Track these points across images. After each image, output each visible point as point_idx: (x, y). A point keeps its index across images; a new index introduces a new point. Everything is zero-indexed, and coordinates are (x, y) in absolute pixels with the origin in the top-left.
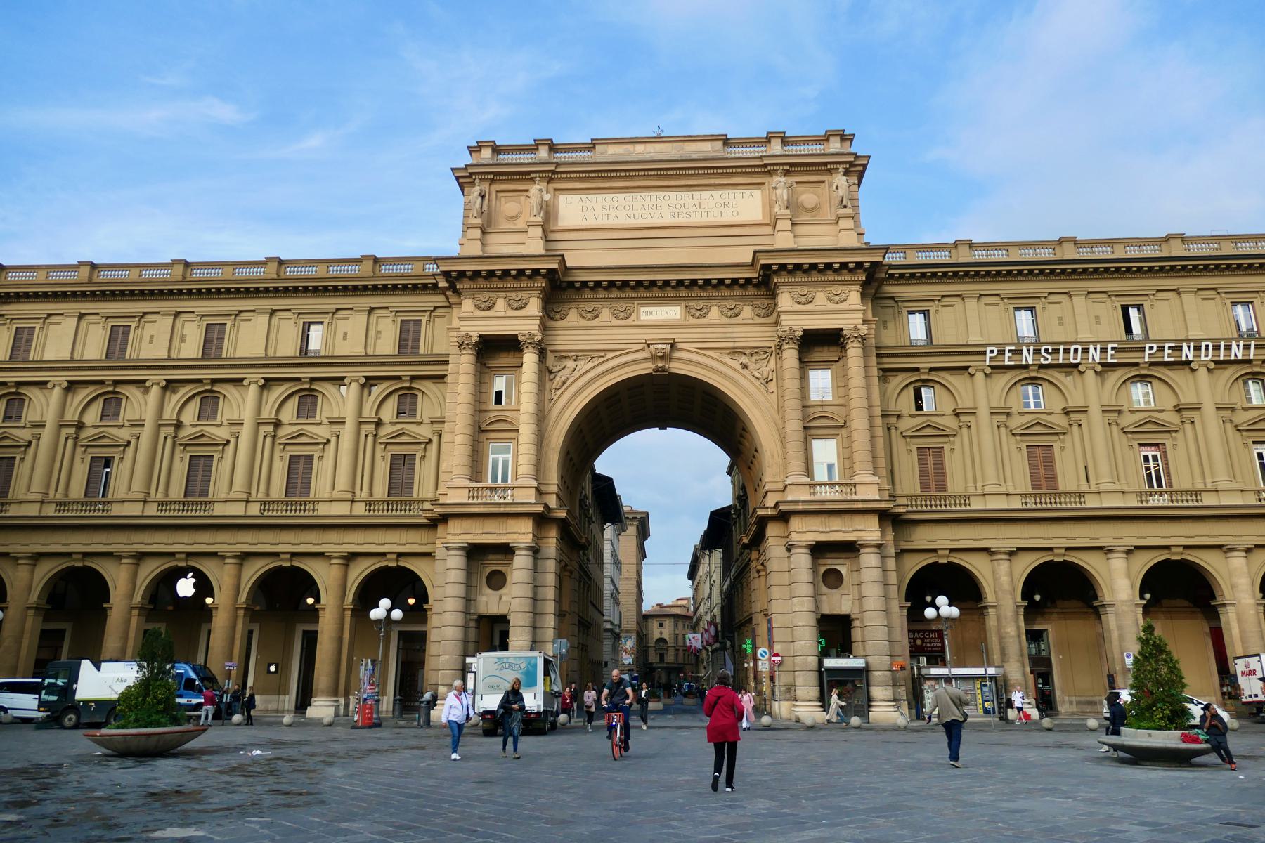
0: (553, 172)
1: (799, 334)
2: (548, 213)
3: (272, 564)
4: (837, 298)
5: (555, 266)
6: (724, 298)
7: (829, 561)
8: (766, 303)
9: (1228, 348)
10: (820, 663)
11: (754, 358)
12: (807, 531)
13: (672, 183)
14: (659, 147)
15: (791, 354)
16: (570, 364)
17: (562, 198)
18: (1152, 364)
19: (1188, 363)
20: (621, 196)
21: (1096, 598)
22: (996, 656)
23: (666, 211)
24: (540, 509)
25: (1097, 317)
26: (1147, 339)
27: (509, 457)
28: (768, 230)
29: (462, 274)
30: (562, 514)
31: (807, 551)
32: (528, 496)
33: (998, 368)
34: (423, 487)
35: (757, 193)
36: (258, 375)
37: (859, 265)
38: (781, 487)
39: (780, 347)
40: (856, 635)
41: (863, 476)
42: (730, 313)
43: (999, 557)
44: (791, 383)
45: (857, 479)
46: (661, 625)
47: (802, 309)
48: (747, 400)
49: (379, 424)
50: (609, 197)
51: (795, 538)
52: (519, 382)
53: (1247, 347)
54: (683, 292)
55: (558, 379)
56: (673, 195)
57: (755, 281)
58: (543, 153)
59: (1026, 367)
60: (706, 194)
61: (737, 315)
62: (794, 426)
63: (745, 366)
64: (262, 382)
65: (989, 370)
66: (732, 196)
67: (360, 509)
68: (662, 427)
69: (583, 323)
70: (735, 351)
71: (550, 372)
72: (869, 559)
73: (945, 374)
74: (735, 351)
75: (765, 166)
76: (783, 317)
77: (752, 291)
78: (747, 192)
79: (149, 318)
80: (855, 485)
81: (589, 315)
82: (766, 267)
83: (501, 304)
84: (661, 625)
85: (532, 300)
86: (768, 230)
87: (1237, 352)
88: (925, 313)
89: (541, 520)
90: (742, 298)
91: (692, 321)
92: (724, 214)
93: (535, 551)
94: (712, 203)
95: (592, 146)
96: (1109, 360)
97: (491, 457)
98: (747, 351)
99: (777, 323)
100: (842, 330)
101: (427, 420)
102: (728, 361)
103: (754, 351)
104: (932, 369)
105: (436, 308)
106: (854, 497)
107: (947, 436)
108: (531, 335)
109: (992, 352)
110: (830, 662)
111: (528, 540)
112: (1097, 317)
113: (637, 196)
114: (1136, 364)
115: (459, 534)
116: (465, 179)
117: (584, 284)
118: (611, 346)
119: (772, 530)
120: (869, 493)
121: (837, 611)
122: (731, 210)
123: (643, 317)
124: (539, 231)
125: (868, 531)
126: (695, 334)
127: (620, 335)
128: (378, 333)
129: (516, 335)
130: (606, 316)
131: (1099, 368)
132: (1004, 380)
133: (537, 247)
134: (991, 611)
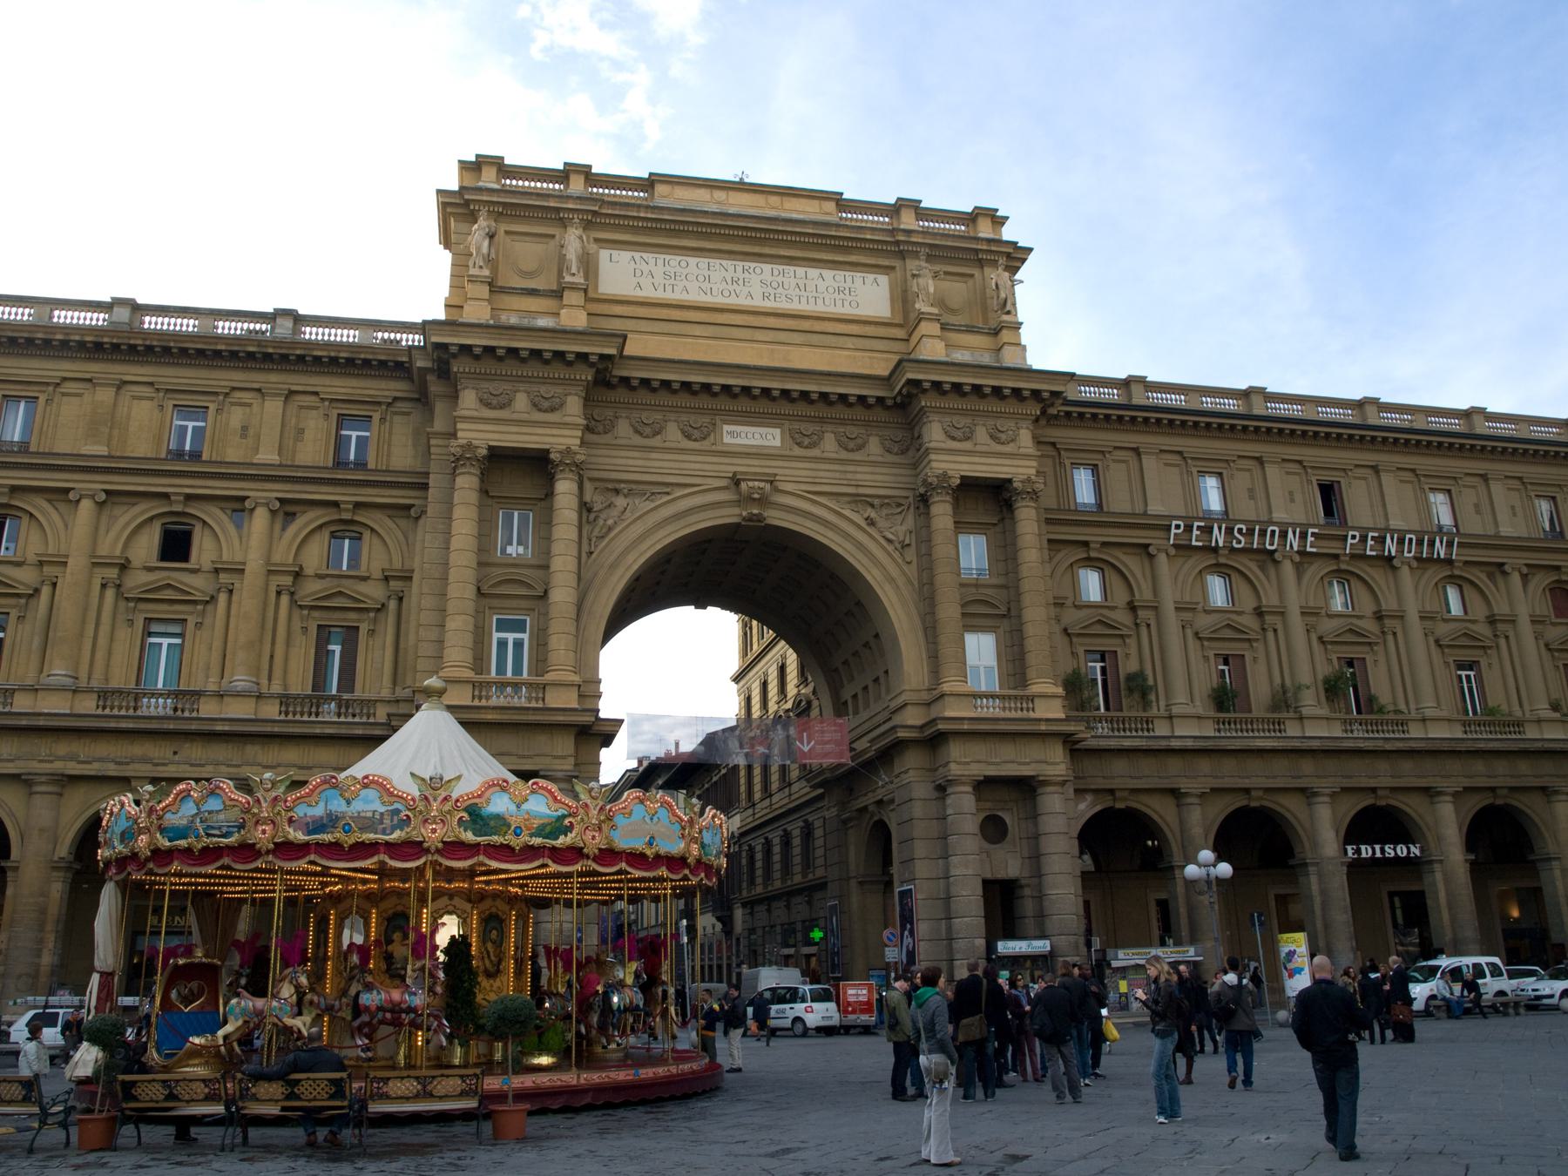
0: (595, 213)
4: (1003, 436)
5: (613, 351)
6: (843, 422)
7: (989, 805)
8: (900, 435)
9: (1432, 544)
10: (991, 947)
11: (885, 511)
13: (767, 250)
15: (942, 511)
16: (620, 502)
17: (604, 254)
18: (1353, 556)
19: (1390, 558)
20: (693, 261)
21: (1292, 855)
22: (1185, 933)
23: (757, 291)
25: (1291, 493)
27: (525, 637)
28: (900, 333)
29: (466, 349)
31: (969, 789)
33: (1184, 548)
35: (883, 280)
36: (97, 484)
38: (925, 696)
39: (924, 501)
40: (1028, 907)
42: (851, 445)
43: (1190, 800)
45: (1034, 689)
47: (956, 452)
48: (875, 572)
49: (298, 575)
50: (674, 260)
51: (955, 770)
52: (546, 522)
54: (786, 408)
55: (601, 522)
56: (767, 267)
57: (890, 402)
58: (577, 186)
59: (1215, 550)
60: (813, 273)
61: (860, 448)
62: (949, 611)
63: (871, 522)
64: (103, 496)
65: (1173, 552)
66: (849, 279)
68: (701, 605)
69: (638, 440)
70: (858, 500)
71: (589, 510)
73: (1118, 553)
74: (858, 500)
75: (898, 243)
76: (933, 457)
77: (880, 414)
78: (871, 277)
80: (1031, 698)
81: (648, 430)
82: (916, 383)
83: (521, 401)
85: (569, 399)
86: (900, 333)
87: (1441, 550)
88: (1095, 469)
90: (867, 424)
91: (798, 451)
92: (839, 303)
94: (822, 288)
96: (1309, 549)
97: (496, 636)
98: (876, 502)
99: (915, 466)
100: (1010, 481)
101: (377, 574)
102: (847, 513)
103: (886, 502)
104: (1104, 544)
105: (395, 399)
106: (1032, 715)
107: (1122, 636)
108: (568, 451)
109: (1178, 527)
112: (1291, 493)
114: (1336, 557)
121: (1001, 875)
123: (727, 439)
125: (1052, 763)
126: (801, 470)
127: (695, 464)
128: (301, 431)
129: (547, 451)
130: (673, 433)
131: (1297, 558)
132: (1195, 563)
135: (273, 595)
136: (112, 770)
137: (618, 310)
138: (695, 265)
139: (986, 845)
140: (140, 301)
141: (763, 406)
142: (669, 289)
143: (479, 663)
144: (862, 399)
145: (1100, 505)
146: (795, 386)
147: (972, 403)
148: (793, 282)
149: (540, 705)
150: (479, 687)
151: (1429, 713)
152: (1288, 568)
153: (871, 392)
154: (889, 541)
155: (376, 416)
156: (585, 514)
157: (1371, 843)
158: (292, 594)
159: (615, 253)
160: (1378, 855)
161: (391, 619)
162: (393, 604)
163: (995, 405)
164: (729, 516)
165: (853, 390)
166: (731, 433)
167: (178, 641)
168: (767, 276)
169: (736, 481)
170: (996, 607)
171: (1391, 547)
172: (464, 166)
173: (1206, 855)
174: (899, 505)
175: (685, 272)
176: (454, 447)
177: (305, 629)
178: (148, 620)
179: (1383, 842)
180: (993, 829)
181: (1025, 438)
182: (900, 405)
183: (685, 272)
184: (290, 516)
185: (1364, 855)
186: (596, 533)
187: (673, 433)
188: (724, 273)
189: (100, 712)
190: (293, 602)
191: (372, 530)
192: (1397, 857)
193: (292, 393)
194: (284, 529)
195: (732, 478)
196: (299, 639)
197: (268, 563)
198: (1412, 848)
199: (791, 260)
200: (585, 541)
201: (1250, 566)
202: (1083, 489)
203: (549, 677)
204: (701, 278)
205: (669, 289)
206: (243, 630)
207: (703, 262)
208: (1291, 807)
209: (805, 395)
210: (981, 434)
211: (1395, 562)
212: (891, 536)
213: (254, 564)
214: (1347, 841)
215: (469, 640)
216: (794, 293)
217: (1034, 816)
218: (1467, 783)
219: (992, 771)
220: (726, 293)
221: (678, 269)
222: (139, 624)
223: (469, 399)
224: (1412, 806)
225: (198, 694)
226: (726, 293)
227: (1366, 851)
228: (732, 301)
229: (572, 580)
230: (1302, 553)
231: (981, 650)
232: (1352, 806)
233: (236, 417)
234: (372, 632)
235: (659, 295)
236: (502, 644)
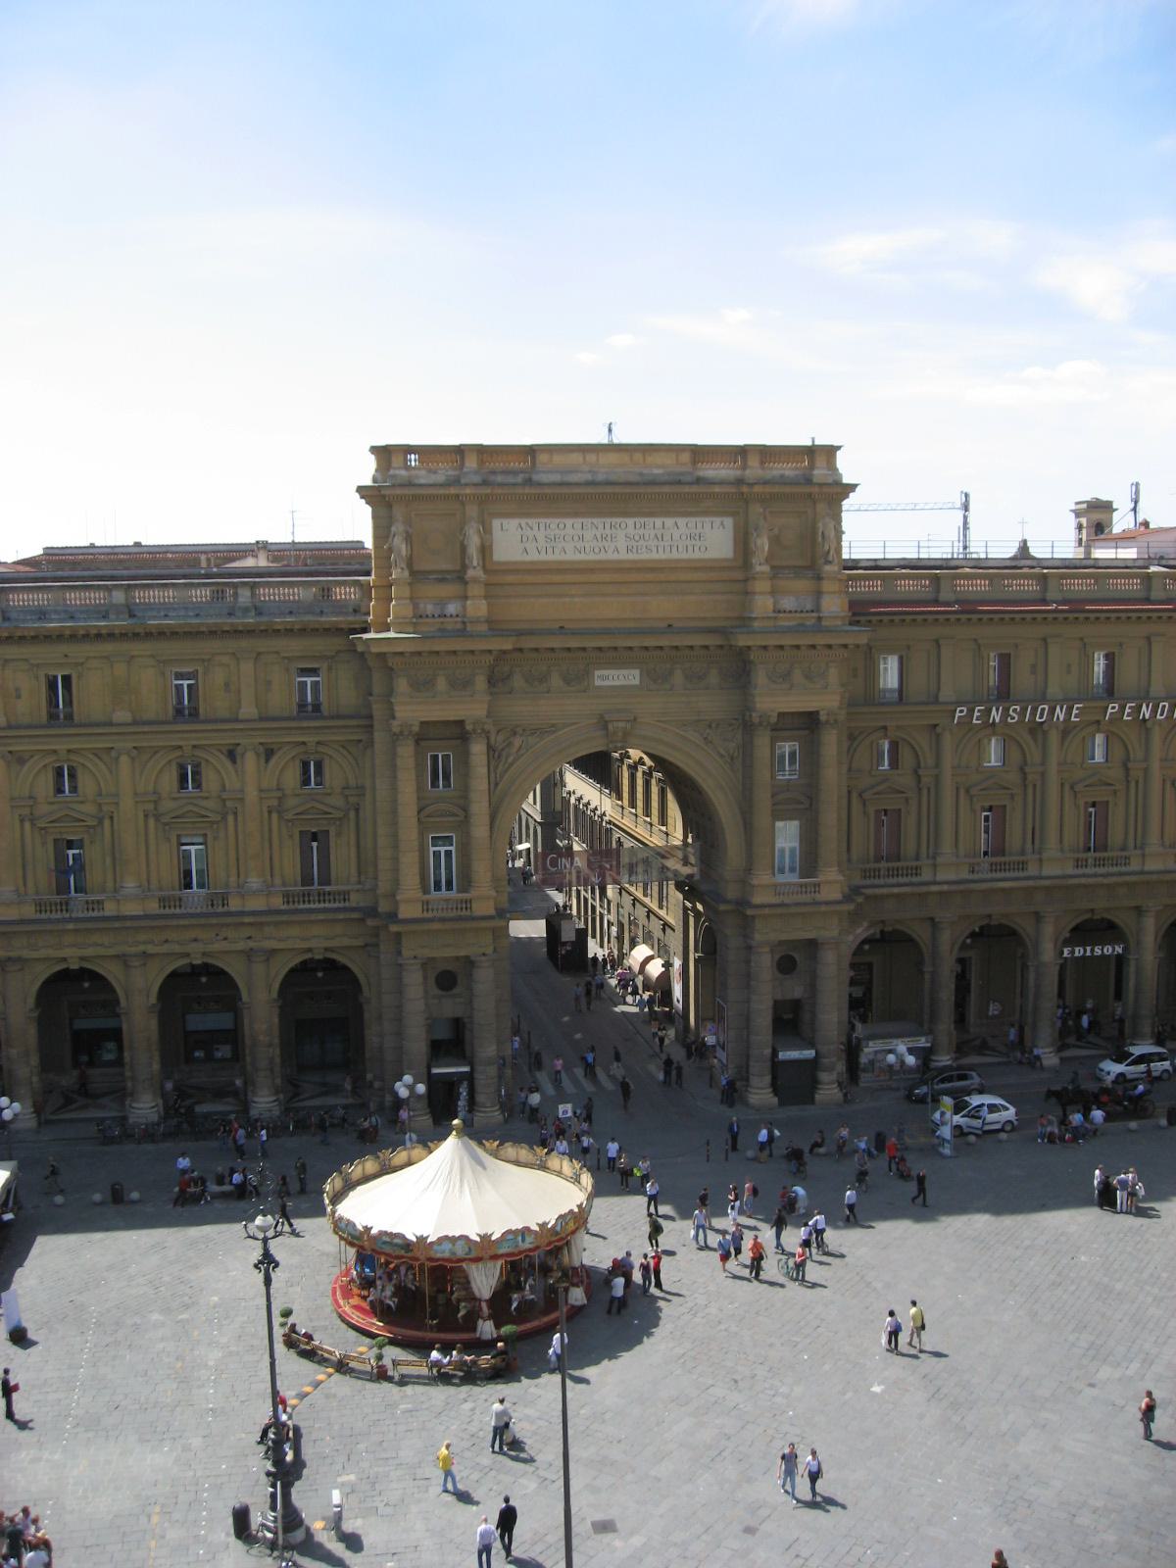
1: (774, 720)
2: (485, 550)
10: (775, 1053)
14: (613, 458)
16: (517, 742)
17: (496, 523)
19: (1144, 720)
20: (569, 522)
23: (622, 544)
25: (1069, 666)
28: (739, 575)
35: (729, 522)
50: (553, 522)
56: (630, 521)
58: (471, 463)
60: (669, 522)
66: (699, 525)
67: (278, 902)
78: (717, 520)
80: (817, 885)
83: (441, 684)
92: (690, 548)
95: (531, 451)
97: (432, 849)
100: (817, 713)
104: (898, 728)
106: (818, 897)
109: (961, 711)
110: (783, 1055)
113: (587, 521)
121: (789, 996)
122: (698, 543)
128: (269, 683)
129: (461, 723)
130: (556, 681)
133: (477, 608)
134: (927, 977)
135: (266, 815)
137: (510, 578)
138: (571, 526)
139: (780, 976)
142: (550, 550)
144: (706, 647)
145: (901, 690)
148: (653, 533)
149: (468, 913)
152: (1054, 737)
153: (712, 641)
154: (722, 756)
155: (325, 666)
156: (491, 753)
157: (1084, 945)
158: (279, 812)
159: (505, 522)
160: (1088, 954)
161: (352, 825)
162: (352, 815)
165: (698, 641)
166: (603, 678)
167: (200, 847)
168: (631, 530)
170: (804, 803)
171: (1145, 711)
172: (374, 450)
174: (730, 725)
175: (563, 533)
176: (395, 725)
177: (291, 836)
178: (179, 836)
179: (1093, 945)
180: (786, 965)
181: (833, 674)
183: (563, 533)
185: (1077, 954)
186: (498, 771)
187: (556, 681)
188: (594, 531)
189: (162, 911)
190: (280, 817)
191: (331, 757)
192: (1103, 956)
193: (259, 654)
194: (267, 761)
195: (602, 717)
198: (1117, 948)
200: (492, 775)
202: (889, 674)
203: (473, 893)
204: (576, 538)
205: (550, 550)
207: (578, 521)
208: (1025, 926)
210: (797, 675)
211: (1149, 724)
212: (723, 752)
213: (252, 794)
214: (1067, 942)
215: (416, 870)
216: (653, 543)
219: (784, 937)
220: (597, 550)
221: (557, 531)
222: (174, 840)
223: (402, 685)
224: (1122, 920)
226: (597, 550)
228: (602, 556)
231: (787, 836)
234: (339, 834)
235: (543, 557)
236: (437, 855)
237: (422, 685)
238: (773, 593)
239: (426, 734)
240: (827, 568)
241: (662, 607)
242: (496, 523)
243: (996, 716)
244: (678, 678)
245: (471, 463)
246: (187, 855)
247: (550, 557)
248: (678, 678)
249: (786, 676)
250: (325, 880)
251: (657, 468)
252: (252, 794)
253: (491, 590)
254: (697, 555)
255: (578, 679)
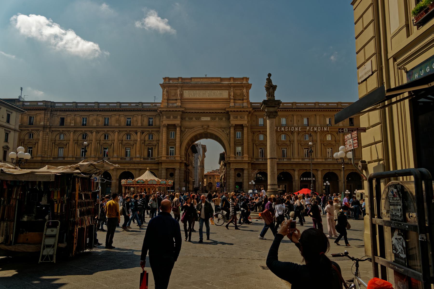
3: (124, 171)
9: (324, 128)
12: (233, 166)
14: (205, 80)
15: (232, 130)
16: (187, 130)
17: (184, 91)
18: (308, 131)
19: (316, 131)
20: (197, 91)
23: (207, 95)
24: (181, 161)
26: (308, 125)
28: (229, 100)
29: (163, 111)
30: (185, 162)
32: (178, 159)
34: (155, 155)
35: (227, 91)
36: (117, 130)
37: (247, 111)
41: (246, 155)
44: (232, 136)
46: (210, 178)
49: (145, 141)
53: (327, 128)
54: (211, 114)
58: (180, 80)
60: (216, 91)
62: (232, 144)
63: (223, 131)
70: (221, 128)
72: (246, 172)
74: (221, 128)
79: (91, 116)
84: (210, 178)
86: (229, 100)
89: (181, 163)
93: (180, 169)
95: (191, 79)
111: (179, 167)
115: (164, 166)
116: (163, 86)
117: (190, 112)
118: (196, 125)
119: (227, 165)
120: (246, 159)
124: (179, 101)
128: (144, 120)
130: (194, 119)
136: (123, 168)
137: (186, 101)
140: (121, 102)
141: (207, 114)
143: (167, 154)
144: (221, 113)
146: (211, 111)
147: (237, 113)
150: (167, 158)
151: (318, 157)
152: (295, 134)
153: (223, 111)
157: (306, 178)
163: (241, 113)
164: (202, 131)
165: (220, 111)
169: (203, 126)
171: (315, 129)
173: (252, 181)
179: (308, 178)
180: (239, 175)
181: (246, 117)
182: (227, 114)
184: (143, 133)
187: (194, 119)
196: (145, 149)
197: (141, 139)
199: (212, 90)
201: (290, 134)
206: (138, 150)
208: (291, 172)
209: (213, 113)
210: (239, 117)
216: (213, 95)
217: (243, 173)
218: (324, 168)
219: (236, 167)
223: (165, 117)
225: (132, 158)
227: (305, 179)
229: (179, 142)
230: (298, 131)
232: (302, 172)
233: (135, 119)
236: (171, 150)
237: (168, 117)
238: (234, 102)
239: (169, 127)
240: (245, 98)
241: (214, 106)
242: (184, 91)
243: (283, 129)
244: (217, 119)
245: (180, 80)
246: (127, 151)
247: (194, 97)
248: (217, 119)
249: (237, 117)
250: (152, 156)
251: (214, 81)
252: (139, 140)
253: (182, 102)
254: (221, 97)
255: (198, 119)
